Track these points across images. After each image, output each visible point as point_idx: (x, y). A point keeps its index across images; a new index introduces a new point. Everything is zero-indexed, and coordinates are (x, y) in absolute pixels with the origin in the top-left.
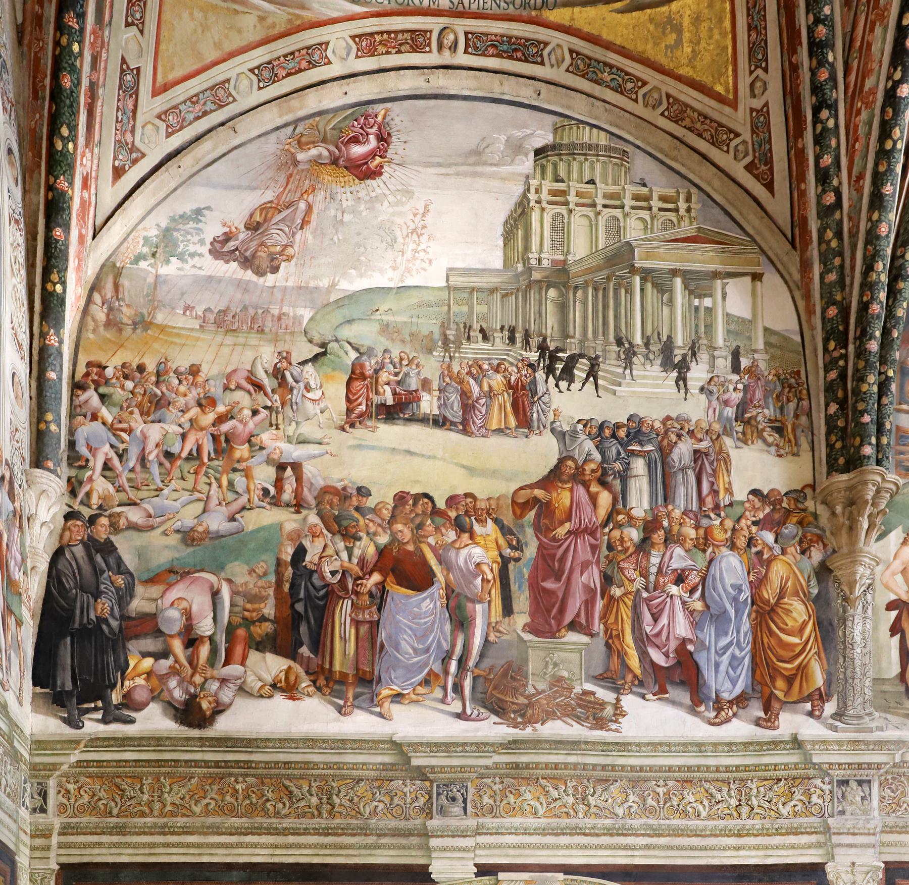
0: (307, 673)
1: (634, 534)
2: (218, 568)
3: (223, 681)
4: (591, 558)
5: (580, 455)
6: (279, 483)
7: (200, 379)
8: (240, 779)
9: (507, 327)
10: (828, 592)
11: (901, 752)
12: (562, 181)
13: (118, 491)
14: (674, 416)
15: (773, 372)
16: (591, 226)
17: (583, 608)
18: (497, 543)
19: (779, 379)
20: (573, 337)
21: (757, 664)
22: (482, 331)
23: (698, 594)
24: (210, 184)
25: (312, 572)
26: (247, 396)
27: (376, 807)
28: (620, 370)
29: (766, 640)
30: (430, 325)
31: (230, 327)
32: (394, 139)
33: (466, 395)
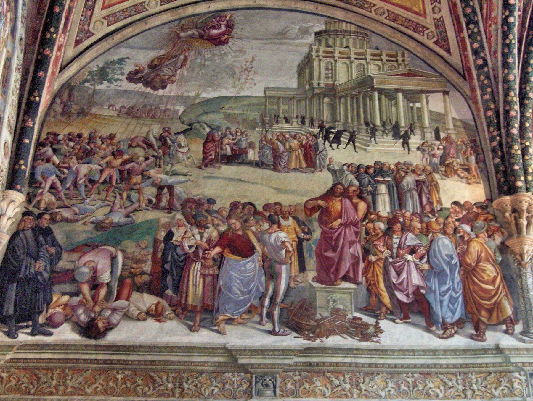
0: (170, 305)
1: (382, 226)
2: (116, 244)
3: (114, 310)
4: (355, 239)
5: (346, 183)
6: (159, 197)
7: (115, 141)
8: (120, 372)
9: (300, 116)
10: (508, 260)
12: (331, 47)
13: (57, 200)
14: (402, 162)
15: (460, 140)
16: (348, 68)
17: (351, 268)
18: (295, 230)
19: (464, 144)
20: (339, 121)
21: (467, 302)
22: (285, 118)
23: (425, 260)
25: (176, 246)
26: (142, 150)
27: (213, 390)
28: (369, 138)
29: (471, 288)
30: (254, 115)
31: (135, 115)
32: (236, 27)
33: (275, 150)
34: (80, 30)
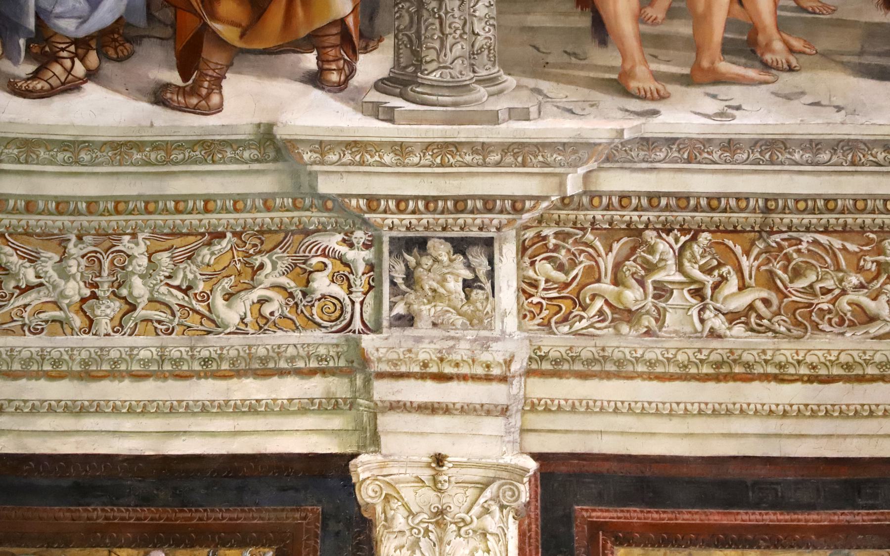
11: (581, 171)
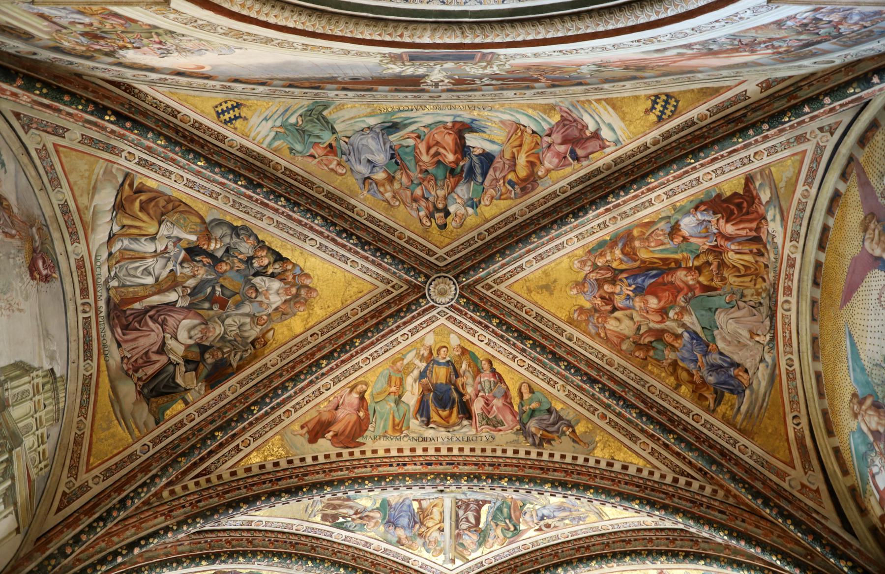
24: (17, 172)
32: (47, 285)
34: (31, 119)
